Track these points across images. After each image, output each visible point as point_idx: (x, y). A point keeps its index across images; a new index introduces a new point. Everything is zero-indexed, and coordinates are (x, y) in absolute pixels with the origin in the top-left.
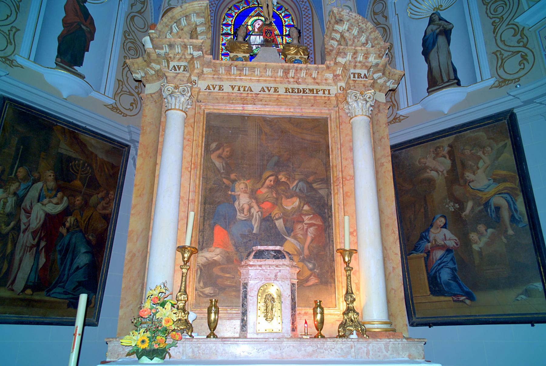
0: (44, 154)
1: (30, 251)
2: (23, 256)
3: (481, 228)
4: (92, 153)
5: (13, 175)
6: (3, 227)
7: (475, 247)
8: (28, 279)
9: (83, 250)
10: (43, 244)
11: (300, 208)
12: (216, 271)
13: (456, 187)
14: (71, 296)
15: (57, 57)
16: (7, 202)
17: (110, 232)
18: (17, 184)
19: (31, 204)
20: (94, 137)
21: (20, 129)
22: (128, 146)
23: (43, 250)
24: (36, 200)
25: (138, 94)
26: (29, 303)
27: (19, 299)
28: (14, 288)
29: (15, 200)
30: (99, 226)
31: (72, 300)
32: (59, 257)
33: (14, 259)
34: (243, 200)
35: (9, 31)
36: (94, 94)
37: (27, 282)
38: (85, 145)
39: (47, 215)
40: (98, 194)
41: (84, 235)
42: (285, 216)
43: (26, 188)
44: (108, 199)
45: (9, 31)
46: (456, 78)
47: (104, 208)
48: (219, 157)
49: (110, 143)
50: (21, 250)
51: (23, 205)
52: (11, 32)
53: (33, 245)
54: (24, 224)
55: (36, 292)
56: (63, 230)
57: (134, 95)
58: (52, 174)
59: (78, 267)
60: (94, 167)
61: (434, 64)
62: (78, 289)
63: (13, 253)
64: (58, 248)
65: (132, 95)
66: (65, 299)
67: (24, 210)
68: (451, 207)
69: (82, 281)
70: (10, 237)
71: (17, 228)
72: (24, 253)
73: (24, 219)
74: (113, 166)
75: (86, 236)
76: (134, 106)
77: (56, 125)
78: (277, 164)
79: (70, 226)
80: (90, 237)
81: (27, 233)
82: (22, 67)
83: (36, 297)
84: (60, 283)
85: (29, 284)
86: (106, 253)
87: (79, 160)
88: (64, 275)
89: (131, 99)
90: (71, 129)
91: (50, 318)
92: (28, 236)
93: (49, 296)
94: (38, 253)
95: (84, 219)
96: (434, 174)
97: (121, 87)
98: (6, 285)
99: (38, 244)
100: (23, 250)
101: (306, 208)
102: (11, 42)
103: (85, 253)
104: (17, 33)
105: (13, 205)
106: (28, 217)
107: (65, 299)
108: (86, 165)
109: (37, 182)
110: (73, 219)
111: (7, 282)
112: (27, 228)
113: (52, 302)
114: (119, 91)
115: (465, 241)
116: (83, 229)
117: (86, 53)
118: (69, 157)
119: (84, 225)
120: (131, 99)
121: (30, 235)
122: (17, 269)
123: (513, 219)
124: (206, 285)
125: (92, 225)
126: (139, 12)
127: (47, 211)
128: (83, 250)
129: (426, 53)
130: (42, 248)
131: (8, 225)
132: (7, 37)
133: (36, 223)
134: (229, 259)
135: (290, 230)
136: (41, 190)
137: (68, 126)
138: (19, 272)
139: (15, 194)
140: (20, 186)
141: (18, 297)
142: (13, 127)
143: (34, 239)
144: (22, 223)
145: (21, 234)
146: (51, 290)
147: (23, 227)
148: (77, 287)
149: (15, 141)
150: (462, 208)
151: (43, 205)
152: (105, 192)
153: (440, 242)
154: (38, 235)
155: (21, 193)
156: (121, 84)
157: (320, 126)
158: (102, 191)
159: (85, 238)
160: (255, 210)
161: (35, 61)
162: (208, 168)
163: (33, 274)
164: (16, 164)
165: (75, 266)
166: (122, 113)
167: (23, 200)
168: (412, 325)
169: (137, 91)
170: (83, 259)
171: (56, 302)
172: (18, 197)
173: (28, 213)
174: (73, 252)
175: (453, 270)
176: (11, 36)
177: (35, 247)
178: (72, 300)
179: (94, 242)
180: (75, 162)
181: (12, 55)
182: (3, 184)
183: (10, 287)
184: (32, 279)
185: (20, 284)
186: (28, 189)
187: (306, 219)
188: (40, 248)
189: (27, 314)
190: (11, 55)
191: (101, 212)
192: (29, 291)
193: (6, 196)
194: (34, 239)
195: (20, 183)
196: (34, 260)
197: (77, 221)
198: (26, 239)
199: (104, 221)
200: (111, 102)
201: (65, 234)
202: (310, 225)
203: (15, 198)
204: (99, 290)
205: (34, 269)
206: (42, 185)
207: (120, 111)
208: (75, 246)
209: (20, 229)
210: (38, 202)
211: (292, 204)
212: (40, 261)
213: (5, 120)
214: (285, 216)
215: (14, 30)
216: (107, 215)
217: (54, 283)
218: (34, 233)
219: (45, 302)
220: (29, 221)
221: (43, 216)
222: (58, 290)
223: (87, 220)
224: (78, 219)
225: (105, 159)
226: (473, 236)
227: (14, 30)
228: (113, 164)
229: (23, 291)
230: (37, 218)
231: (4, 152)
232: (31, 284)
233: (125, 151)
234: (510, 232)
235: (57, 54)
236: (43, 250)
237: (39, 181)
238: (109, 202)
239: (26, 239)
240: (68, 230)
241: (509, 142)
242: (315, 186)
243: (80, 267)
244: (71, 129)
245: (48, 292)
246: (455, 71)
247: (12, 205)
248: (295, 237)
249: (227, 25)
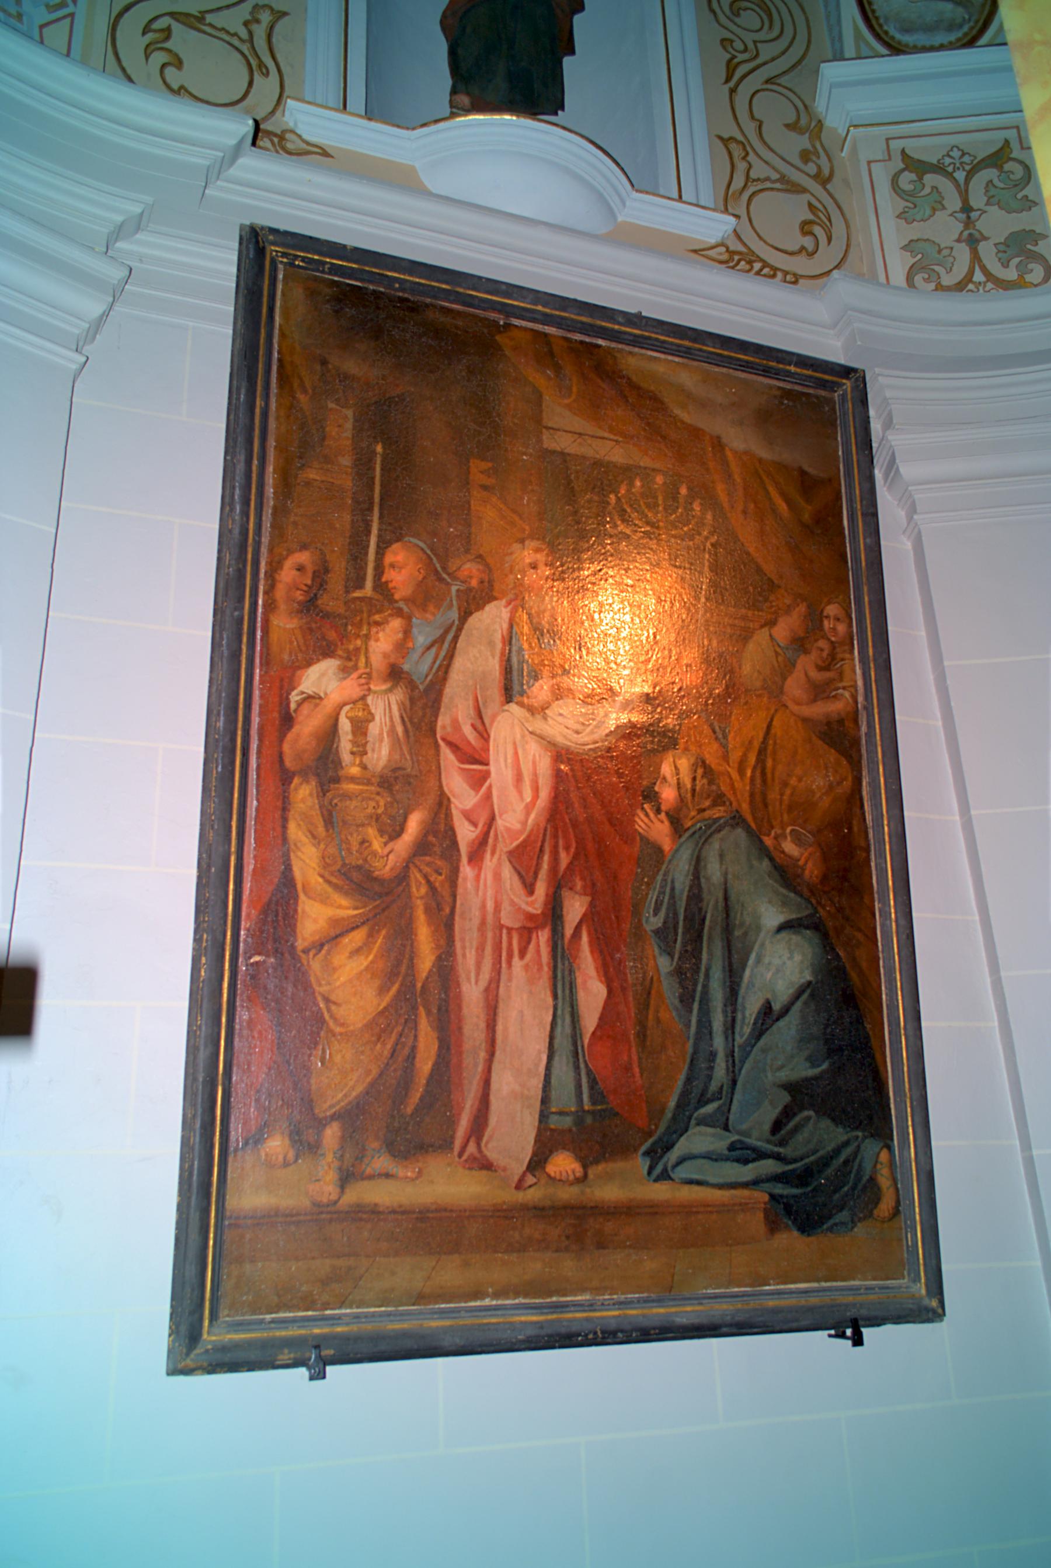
0: (485, 465)
1: (522, 954)
2: (495, 982)
4: (696, 433)
5: (369, 584)
6: (377, 845)
8: (545, 1101)
9: (771, 916)
10: (575, 908)
14: (769, 1166)
15: (454, 91)
16: (371, 718)
17: (876, 806)
18: (396, 623)
19: (480, 716)
20: (686, 353)
21: (351, 366)
22: (847, 372)
23: (585, 938)
24: (495, 693)
25: (824, 180)
26: (580, 1226)
27: (525, 1208)
28: (491, 1152)
29: (402, 705)
30: (818, 782)
31: (779, 1189)
32: (665, 965)
33: (459, 996)
35: (246, 24)
37: (543, 1116)
38: (655, 398)
40: (772, 623)
41: (755, 837)
43: (440, 640)
44: (822, 643)
45: (246, 24)
47: (819, 692)
49: (766, 372)
50: (481, 949)
51: (443, 721)
52: (254, 27)
53: (530, 917)
54: (468, 816)
55: (597, 1162)
56: (655, 828)
57: (804, 190)
58: (541, 557)
59: (767, 1009)
60: (723, 498)
62: (796, 1129)
63: (446, 969)
64: (654, 922)
65: (796, 189)
66: (745, 1185)
67: (454, 747)
69: (807, 1080)
70: (419, 890)
71: (439, 839)
72: (497, 971)
73: (462, 796)
74: (807, 484)
75: (768, 841)
76: (817, 230)
77: (508, 326)
79: (681, 799)
80: (789, 847)
81: (489, 863)
82: (325, 154)
83: (609, 1192)
84: (702, 1101)
85: (554, 1122)
86: (886, 915)
87: (647, 474)
88: (713, 1055)
89: (796, 209)
90: (578, 337)
91: (700, 1299)
92: (497, 876)
93: (665, 1176)
94: (561, 956)
95: (735, 756)
97: (741, 166)
98: (446, 1145)
99: (554, 913)
100: (489, 949)
102: (261, 65)
103: (781, 928)
104: (278, 28)
105: (400, 729)
106: (479, 780)
107: (745, 1185)
108: (684, 491)
109: (480, 607)
110: (684, 764)
111: (452, 1123)
112: (486, 835)
113: (688, 1210)
114: (738, 182)
116: (745, 807)
117: (567, 61)
118: (597, 464)
119: (743, 787)
120: (796, 209)
121: (507, 872)
122: (483, 1055)
125: (785, 784)
127: (560, 740)
128: (771, 916)
130: (578, 929)
131: (397, 832)
132: (245, 48)
133: (520, 807)
136: (509, 640)
137: (558, 322)
138: (496, 1066)
139: (395, 674)
140: (407, 632)
141: (521, 1197)
142: (324, 362)
143: (530, 890)
144: (455, 812)
145: (467, 871)
146: (669, 1147)
147: (466, 833)
148: (787, 1113)
149: (341, 425)
151: (531, 710)
152: (802, 608)
154: (545, 866)
155: (420, 666)
156: (737, 152)
158: (788, 610)
159: (765, 852)
161: (369, 115)
163: (563, 1071)
164: (368, 533)
165: (751, 1006)
166: (776, 270)
167: (440, 693)
169: (811, 168)
170: (781, 966)
171: (707, 1206)
172: (412, 685)
173: (474, 758)
174: (728, 930)
176: (260, 43)
177: (542, 927)
178: (779, 1189)
179: (812, 871)
180: (631, 484)
181: (278, 114)
182: (332, 635)
183: (472, 1148)
184: (564, 1096)
185: (513, 1133)
186: (447, 644)
188: (569, 932)
189: (583, 1290)
190: (273, 112)
191: (807, 711)
192: (563, 1164)
193: (356, 692)
194: (530, 890)
195: (409, 618)
196: (555, 996)
197: (708, 771)
198: (491, 890)
199: (832, 755)
200: (716, 227)
201: (667, 845)
203: (397, 697)
204: (902, 1119)
205: (563, 1043)
206: (506, 614)
207: (765, 264)
208: (726, 899)
209: (454, 843)
210: (508, 698)
212: (581, 995)
213: (282, 335)
215: (266, 17)
216: (841, 722)
217: (672, 1104)
218: (525, 859)
219: (653, 1210)
220: (488, 796)
221: (545, 765)
222: (700, 1139)
223: (752, 759)
224: (711, 760)
225: (764, 454)
227: (266, 17)
228: (803, 473)
229: (537, 1163)
230: (519, 778)
231: (308, 483)
232: (567, 1122)
233: (843, 397)
235: (448, 82)
236: (585, 938)
237: (492, 598)
238: (833, 656)
239: (491, 890)
240: (675, 821)
243: (777, 1007)
244: (578, 337)
245: (655, 1154)
247: (392, 730)
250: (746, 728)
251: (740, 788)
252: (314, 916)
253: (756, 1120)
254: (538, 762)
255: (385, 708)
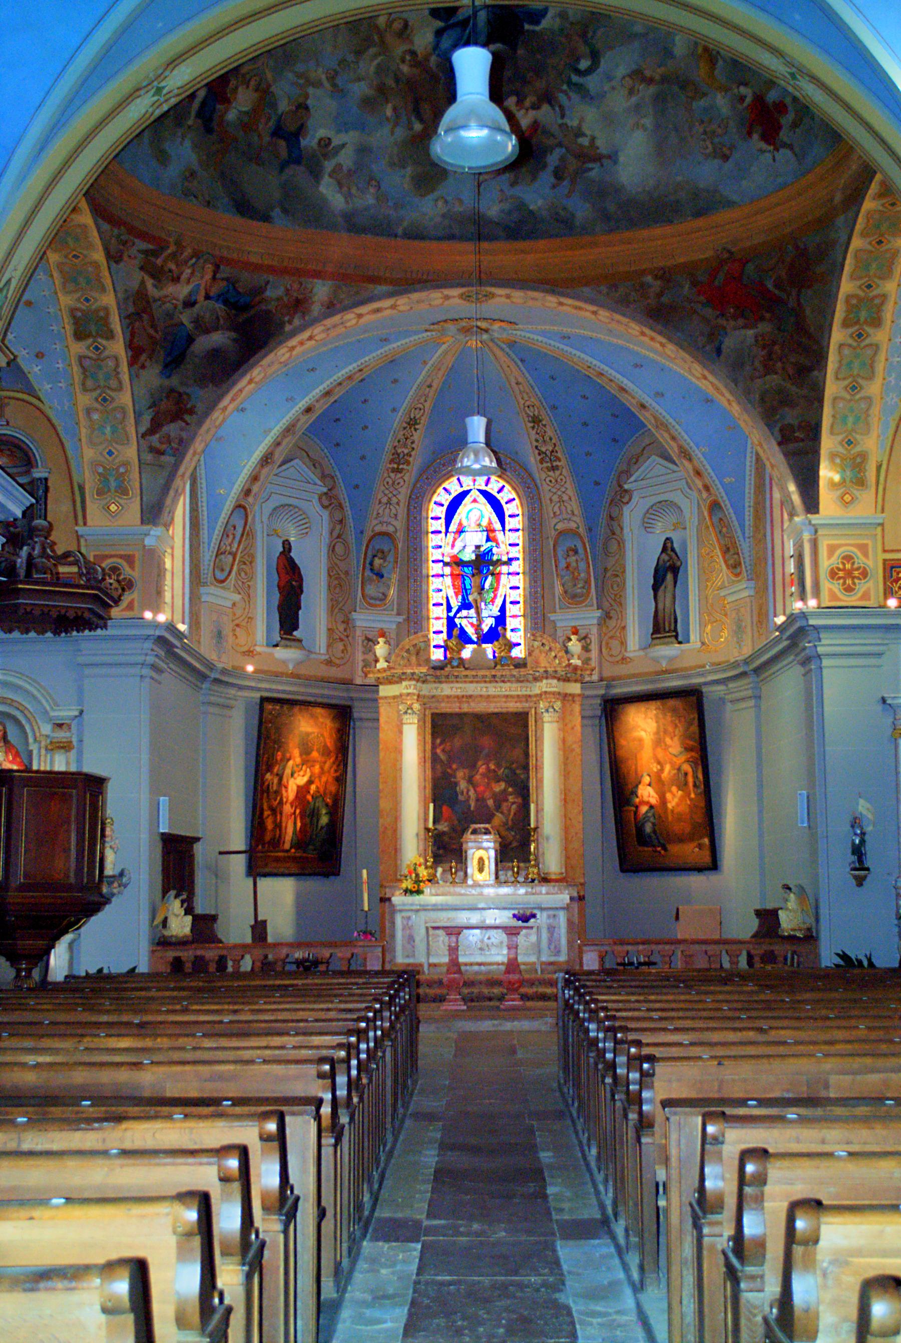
3: (674, 789)
7: (670, 806)
10: (298, 811)
11: (505, 790)
12: (446, 839)
13: (659, 750)
34: (463, 785)
36: (313, 656)
39: (298, 787)
42: (495, 796)
46: (675, 630)
48: (443, 750)
56: (309, 797)
61: (661, 606)
68: (655, 768)
73: (284, 794)
78: (488, 755)
96: (643, 734)
101: (510, 790)
115: (663, 801)
123: (695, 786)
124: (438, 849)
126: (339, 537)
129: (656, 588)
134: (453, 829)
135: (498, 807)
150: (662, 770)
153: (646, 799)
157: (521, 720)
160: (472, 793)
162: (435, 759)
168: (623, 870)
170: (324, 820)
173: (286, 787)
175: (654, 824)
185: (287, 846)
186: (284, 769)
187: (511, 799)
198: (287, 809)
200: (327, 657)
202: (513, 803)
211: (499, 787)
214: (495, 796)
218: (292, 804)
222: (311, 847)
226: (668, 796)
234: (693, 796)
241: (696, 716)
242: (518, 772)
246: (676, 622)
248: (502, 813)
249: (437, 518)
250: (324, 779)
251: (322, 790)
252: (266, 813)
253: (318, 844)
254: (295, 788)
255: (276, 781)
